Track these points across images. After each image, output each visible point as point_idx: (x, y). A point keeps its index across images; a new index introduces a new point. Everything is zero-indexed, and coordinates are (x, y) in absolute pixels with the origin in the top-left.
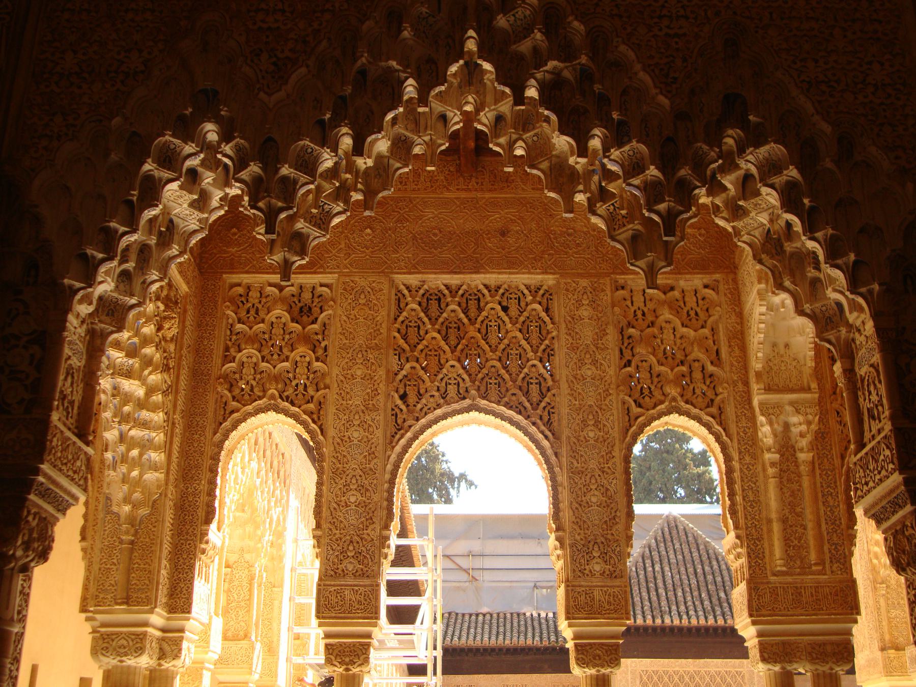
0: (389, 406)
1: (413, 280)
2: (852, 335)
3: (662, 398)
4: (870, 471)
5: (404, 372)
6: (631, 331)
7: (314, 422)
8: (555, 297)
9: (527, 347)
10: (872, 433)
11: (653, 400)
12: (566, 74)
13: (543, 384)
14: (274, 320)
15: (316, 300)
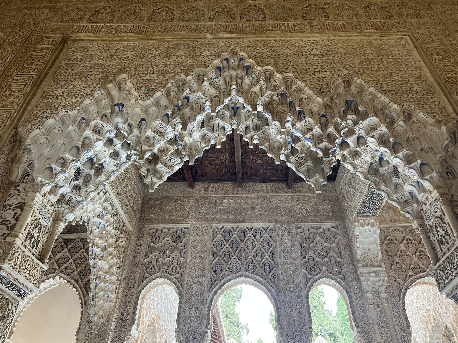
0: (209, 275)
1: (219, 226)
2: (420, 207)
3: (320, 271)
4: (448, 270)
5: (215, 261)
6: (305, 244)
7: (179, 282)
8: (274, 232)
9: (264, 251)
10: (443, 252)
11: (316, 272)
12: (275, 98)
13: (271, 266)
14: (166, 242)
15: (182, 234)
